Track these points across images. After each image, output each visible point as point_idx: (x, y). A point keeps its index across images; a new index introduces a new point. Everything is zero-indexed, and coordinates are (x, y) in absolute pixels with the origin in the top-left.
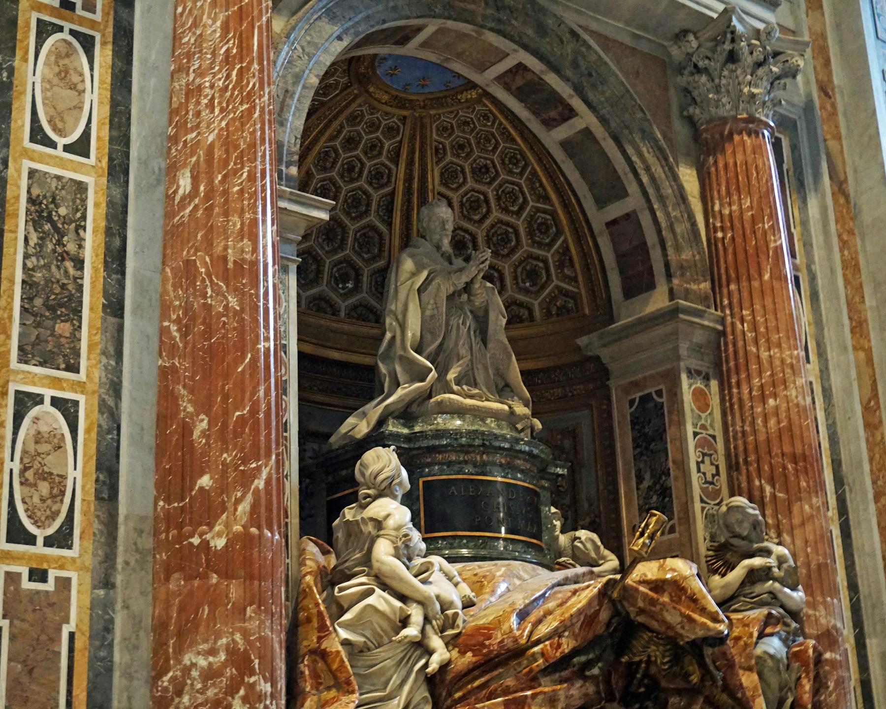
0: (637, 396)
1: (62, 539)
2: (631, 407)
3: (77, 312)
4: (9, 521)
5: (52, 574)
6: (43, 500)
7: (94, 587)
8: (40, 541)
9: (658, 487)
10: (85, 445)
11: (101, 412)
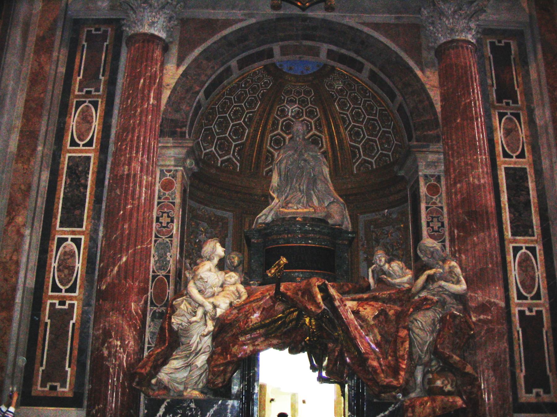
1: (72, 289)
4: (52, 285)
5: (68, 302)
6: (65, 276)
7: (84, 306)
8: (64, 291)
11: (90, 241)
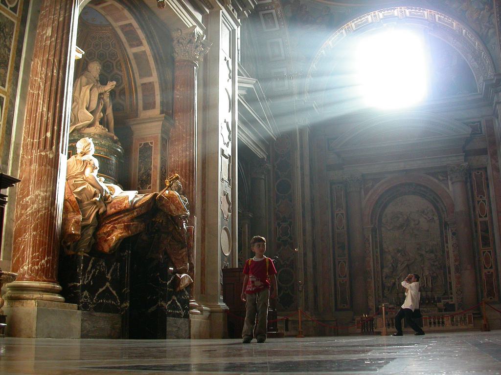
0: (143, 143)
2: (140, 145)
3: (7, 66)
9: (146, 173)
10: (4, 114)
